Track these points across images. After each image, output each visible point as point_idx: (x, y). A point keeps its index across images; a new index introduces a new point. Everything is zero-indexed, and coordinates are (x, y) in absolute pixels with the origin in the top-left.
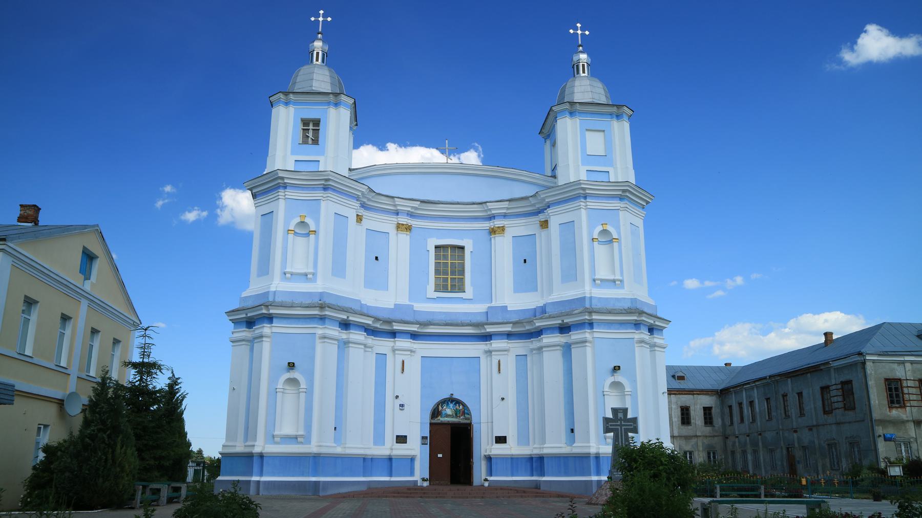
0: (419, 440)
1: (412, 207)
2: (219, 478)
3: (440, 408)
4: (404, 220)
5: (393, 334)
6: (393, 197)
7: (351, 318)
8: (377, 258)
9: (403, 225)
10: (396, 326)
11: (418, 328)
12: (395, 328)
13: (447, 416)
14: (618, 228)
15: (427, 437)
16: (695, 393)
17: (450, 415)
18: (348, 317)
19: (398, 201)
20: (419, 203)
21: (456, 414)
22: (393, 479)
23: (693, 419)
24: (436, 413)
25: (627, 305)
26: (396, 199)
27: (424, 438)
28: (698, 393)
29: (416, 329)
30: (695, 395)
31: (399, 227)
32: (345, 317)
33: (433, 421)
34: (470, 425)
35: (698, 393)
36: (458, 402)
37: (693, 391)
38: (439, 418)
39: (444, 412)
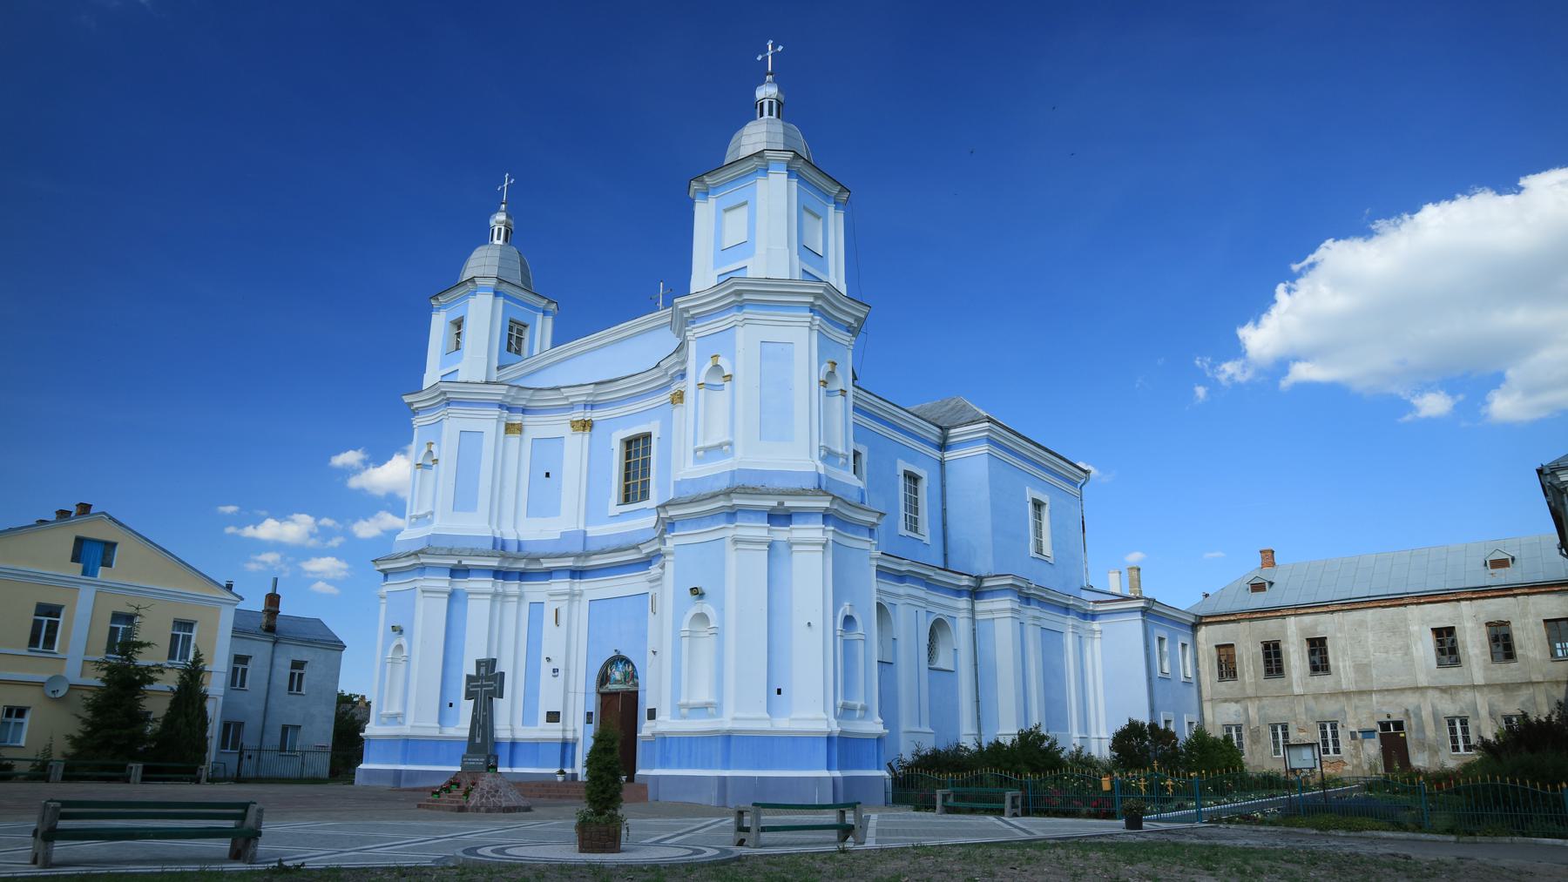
0: (581, 718)
1: (589, 395)
2: (361, 766)
3: (609, 671)
4: (579, 415)
5: (549, 574)
7: (464, 563)
8: (548, 475)
9: (578, 421)
10: (546, 563)
11: (573, 561)
12: (545, 565)
13: (617, 682)
14: (733, 358)
15: (592, 713)
16: (1516, 591)
17: (618, 681)
18: (460, 562)
19: (566, 392)
20: (592, 386)
21: (625, 679)
22: (516, 770)
23: (1521, 647)
24: (604, 678)
25: (723, 484)
26: (562, 390)
27: (589, 715)
28: (1526, 591)
29: (571, 564)
30: (1519, 597)
31: (573, 424)
32: (456, 562)
33: (601, 690)
34: (636, 693)
35: (1526, 591)
36: (627, 661)
37: (1511, 589)
38: (608, 685)
39: (613, 677)
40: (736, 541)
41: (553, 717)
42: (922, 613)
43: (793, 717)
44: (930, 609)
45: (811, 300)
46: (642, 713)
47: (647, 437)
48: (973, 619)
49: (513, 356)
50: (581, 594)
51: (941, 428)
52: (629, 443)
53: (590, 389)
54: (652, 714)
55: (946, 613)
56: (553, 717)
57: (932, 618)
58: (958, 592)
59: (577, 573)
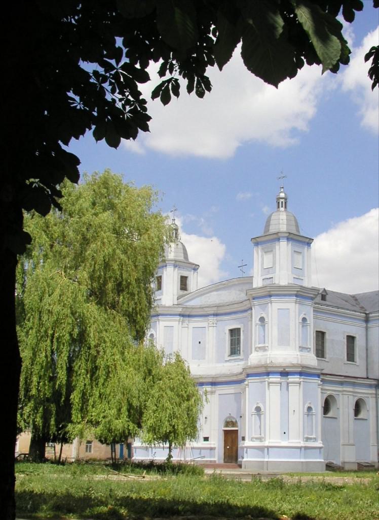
6: (203, 308)
8: (200, 343)
19: (206, 309)
40: (269, 383)
41: (206, 439)
42: (351, 397)
43: (290, 441)
44: (355, 395)
45: (296, 293)
46: (240, 438)
47: (239, 330)
48: (376, 397)
49: (182, 292)
50: (215, 392)
51: (366, 314)
52: (231, 331)
53: (215, 309)
54: (243, 439)
55: (362, 395)
56: (206, 439)
57: (356, 399)
58: (370, 386)
59: (213, 384)
